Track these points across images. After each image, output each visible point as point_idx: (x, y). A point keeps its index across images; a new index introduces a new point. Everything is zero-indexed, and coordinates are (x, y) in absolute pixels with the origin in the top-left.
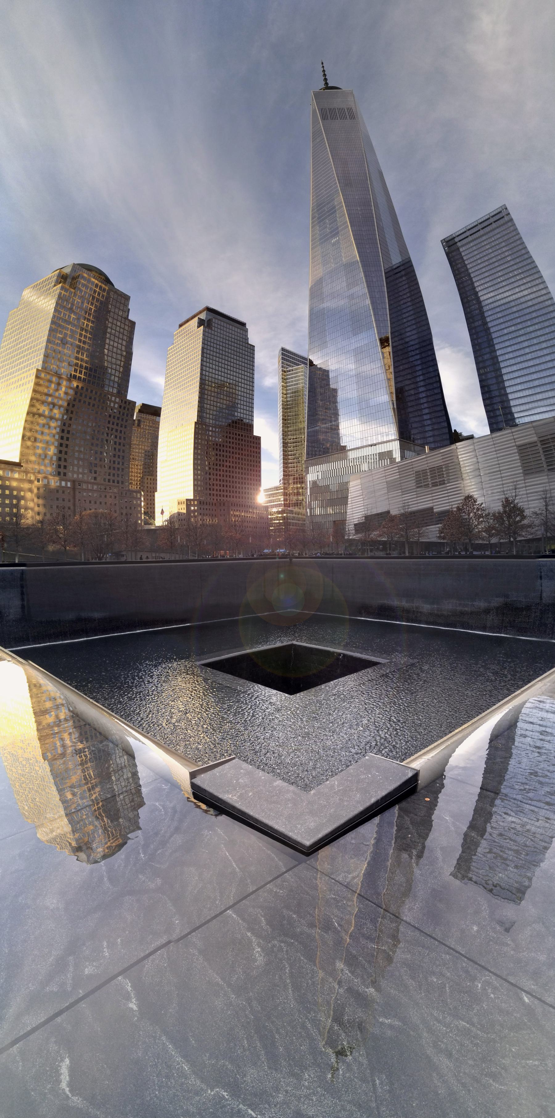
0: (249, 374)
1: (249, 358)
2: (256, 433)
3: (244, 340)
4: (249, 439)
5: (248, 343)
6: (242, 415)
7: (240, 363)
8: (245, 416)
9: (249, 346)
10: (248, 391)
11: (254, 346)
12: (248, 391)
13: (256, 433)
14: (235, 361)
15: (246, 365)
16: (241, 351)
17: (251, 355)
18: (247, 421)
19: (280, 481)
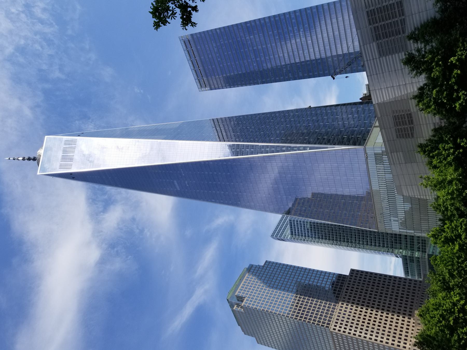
0: (291, 270)
1: (276, 268)
2: (347, 273)
3: (260, 270)
4: (352, 280)
5: (263, 266)
6: (328, 283)
7: (280, 276)
8: (329, 280)
9: (266, 266)
10: (306, 273)
11: (266, 261)
12: (306, 273)
13: (347, 273)
14: (278, 281)
15: (282, 271)
16: (269, 274)
17: (274, 265)
18: (334, 279)
19: (398, 257)
